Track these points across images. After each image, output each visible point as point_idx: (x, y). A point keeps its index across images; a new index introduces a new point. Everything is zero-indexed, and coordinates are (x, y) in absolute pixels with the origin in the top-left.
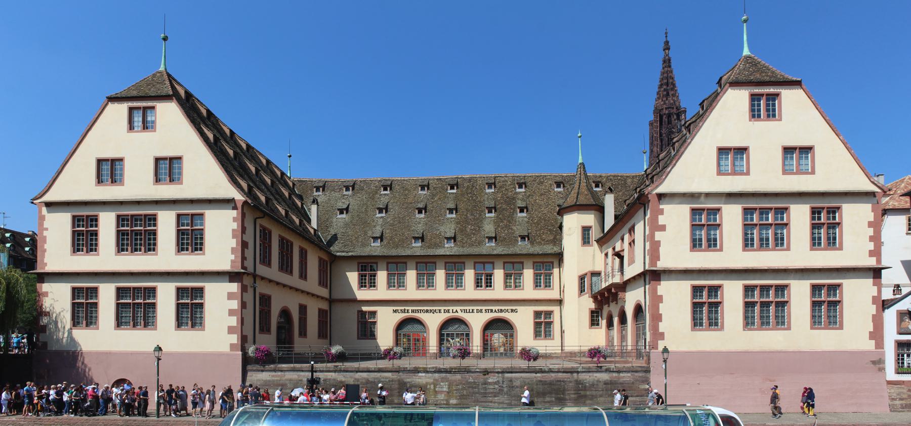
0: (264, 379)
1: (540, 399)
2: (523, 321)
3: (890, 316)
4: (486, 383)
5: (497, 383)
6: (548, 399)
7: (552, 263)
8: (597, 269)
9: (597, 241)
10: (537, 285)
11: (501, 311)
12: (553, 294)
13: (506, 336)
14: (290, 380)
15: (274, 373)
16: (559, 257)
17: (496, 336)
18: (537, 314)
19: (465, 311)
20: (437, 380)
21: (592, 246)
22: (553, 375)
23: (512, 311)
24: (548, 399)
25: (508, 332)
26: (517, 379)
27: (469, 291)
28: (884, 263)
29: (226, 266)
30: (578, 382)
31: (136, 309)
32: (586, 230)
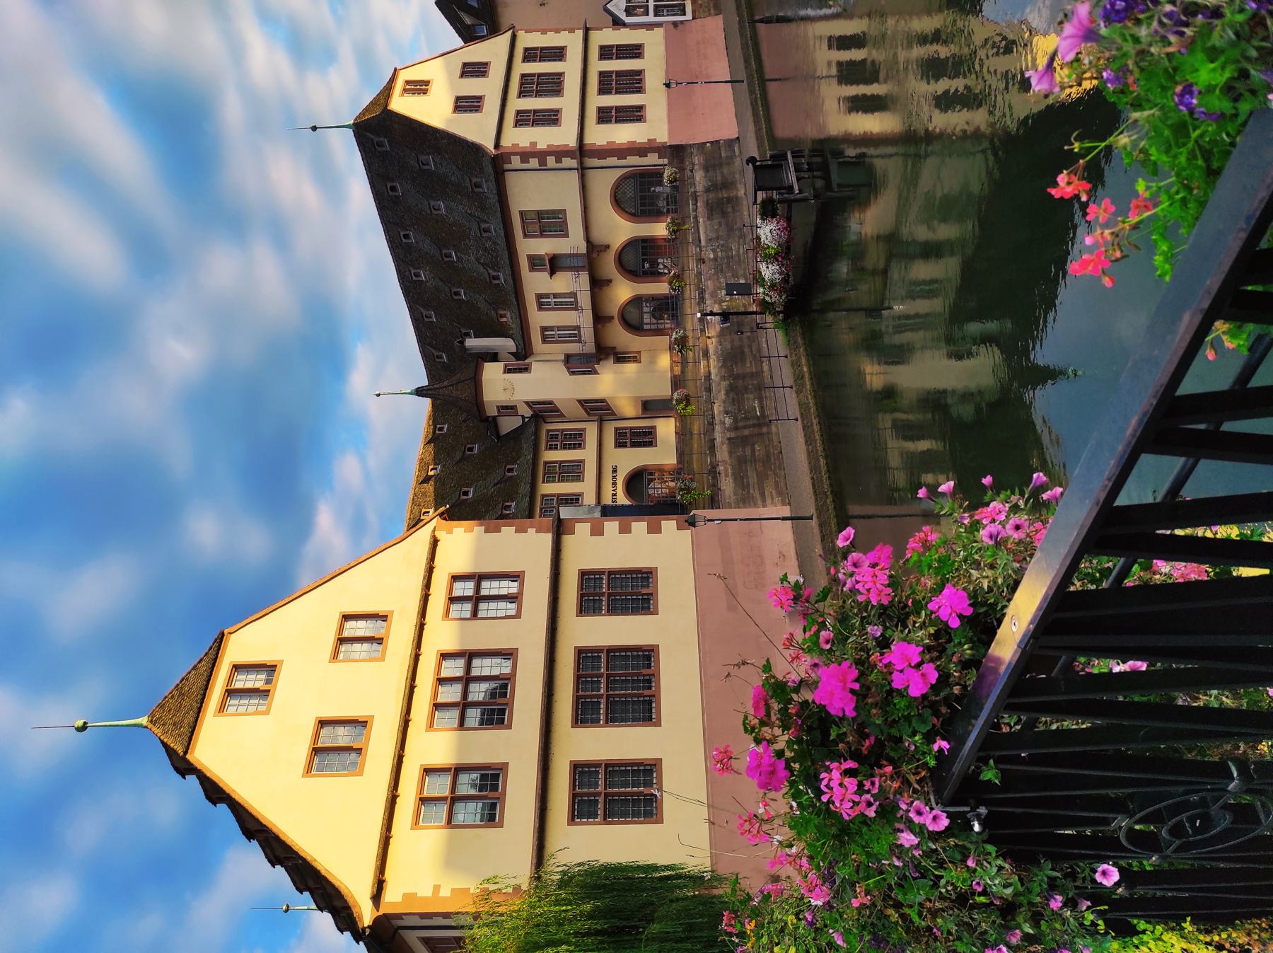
2: (629, 460)
4: (715, 259)
5: (714, 251)
6: (730, 210)
7: (548, 431)
9: (525, 358)
10: (579, 446)
11: (614, 483)
12: (591, 431)
13: (652, 480)
14: (730, 453)
16: (543, 411)
17: (650, 492)
18: (620, 444)
21: (529, 365)
22: (700, 210)
23: (615, 470)
24: (730, 210)
25: (647, 477)
28: (582, 25)
29: (547, 538)
30: (707, 190)
32: (508, 370)
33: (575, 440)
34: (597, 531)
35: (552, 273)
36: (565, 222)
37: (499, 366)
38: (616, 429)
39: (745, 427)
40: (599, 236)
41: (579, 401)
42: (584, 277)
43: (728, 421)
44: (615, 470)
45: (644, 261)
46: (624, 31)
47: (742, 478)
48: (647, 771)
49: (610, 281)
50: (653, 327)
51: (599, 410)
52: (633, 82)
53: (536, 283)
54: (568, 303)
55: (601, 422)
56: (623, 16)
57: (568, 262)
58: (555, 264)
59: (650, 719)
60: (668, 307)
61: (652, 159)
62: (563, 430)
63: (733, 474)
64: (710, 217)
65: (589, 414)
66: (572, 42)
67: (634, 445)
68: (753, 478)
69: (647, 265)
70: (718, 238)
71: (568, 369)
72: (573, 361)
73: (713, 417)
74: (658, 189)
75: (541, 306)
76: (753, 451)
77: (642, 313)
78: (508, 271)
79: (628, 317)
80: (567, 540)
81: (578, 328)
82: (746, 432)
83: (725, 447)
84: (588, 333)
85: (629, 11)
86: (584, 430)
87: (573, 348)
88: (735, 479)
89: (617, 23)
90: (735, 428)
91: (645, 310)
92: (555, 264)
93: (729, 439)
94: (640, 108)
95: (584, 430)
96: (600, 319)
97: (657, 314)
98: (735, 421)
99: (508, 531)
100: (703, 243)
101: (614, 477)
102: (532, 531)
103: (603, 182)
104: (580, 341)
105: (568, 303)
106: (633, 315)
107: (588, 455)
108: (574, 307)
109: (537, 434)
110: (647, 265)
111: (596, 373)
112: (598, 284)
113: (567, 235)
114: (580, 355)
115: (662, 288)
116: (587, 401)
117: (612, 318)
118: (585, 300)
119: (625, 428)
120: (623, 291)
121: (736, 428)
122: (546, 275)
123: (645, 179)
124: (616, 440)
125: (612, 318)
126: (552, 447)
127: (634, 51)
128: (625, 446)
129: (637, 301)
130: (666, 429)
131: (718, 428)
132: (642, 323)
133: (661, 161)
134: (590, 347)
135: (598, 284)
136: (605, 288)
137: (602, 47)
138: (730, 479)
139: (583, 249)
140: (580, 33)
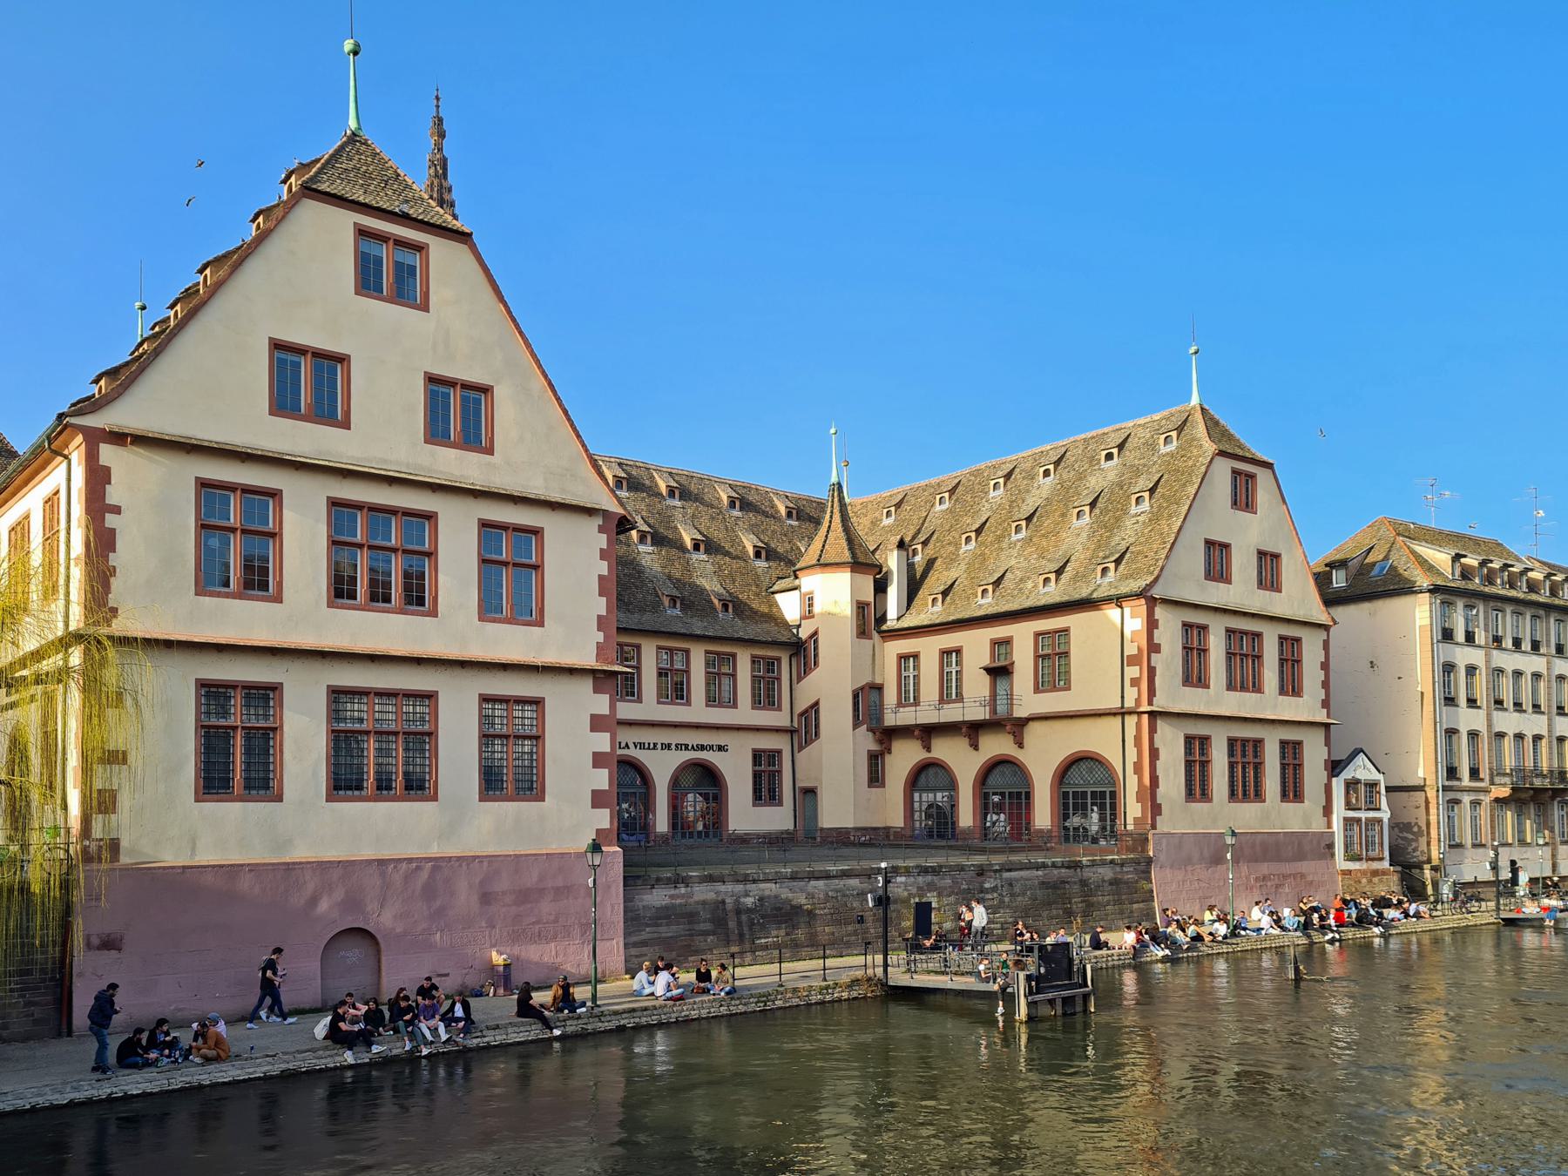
0: (658, 904)
1: (1045, 914)
3: (1338, 786)
5: (994, 889)
7: (779, 660)
8: (878, 681)
9: (880, 632)
11: (702, 748)
12: (780, 718)
13: (706, 797)
14: (704, 903)
15: (673, 892)
17: (690, 797)
18: (757, 756)
19: (642, 746)
20: (920, 888)
22: (1056, 872)
23: (721, 748)
25: (711, 791)
26: (1017, 880)
27: (649, 707)
30: (1084, 883)
31: (379, 753)
33: (765, 696)
34: (597, 723)
35: (989, 670)
36: (1054, 689)
37: (868, 595)
38: (779, 752)
39: (740, 923)
40: (1033, 732)
41: (817, 703)
42: (980, 714)
43: (749, 901)
44: (721, 748)
45: (1003, 794)
46: (1323, 775)
47: (668, 917)
48: (262, 782)
49: (976, 748)
50: (916, 805)
51: (806, 727)
52: (1246, 788)
53: (976, 646)
54: (950, 691)
55: (791, 732)
56: (1348, 774)
57: (1001, 690)
58: (999, 672)
59: (337, 788)
60: (941, 825)
61: (1133, 810)
62: (779, 679)
63: (674, 906)
64: (1044, 884)
65: (801, 715)
66: (1306, 707)
67: (757, 776)
68: (666, 931)
69: (996, 799)
70: (1012, 895)
71: (862, 688)
72: (874, 695)
73: (754, 881)
74: (1095, 816)
75: (946, 653)
76: (706, 933)
77: (934, 790)
78: (991, 611)
79: (931, 771)
80: (587, 684)
81: (917, 703)
82: (732, 924)
83: (711, 896)
84: (906, 717)
85: (1351, 785)
86: (779, 709)
87: (890, 696)
88: (666, 908)
89: (1335, 767)
90: (738, 912)
91: (939, 795)
92: (999, 672)
93: (723, 902)
94: (1205, 796)
95: (779, 709)
96: (928, 733)
97: (934, 811)
98: (749, 910)
99: (601, 606)
100: (1006, 875)
101: (711, 747)
102: (600, 637)
103: (1103, 740)
104: (900, 704)
105: (950, 691)
106: (930, 777)
107: (744, 713)
108: (944, 699)
109: (775, 644)
110: (996, 799)
111: (856, 725)
112: (973, 731)
113: (1037, 690)
114: (882, 704)
115: (966, 817)
116: (817, 712)
117: (929, 750)
118: (952, 714)
119: (780, 764)
120: (964, 761)
121: (738, 912)
122: (986, 661)
123: (1108, 801)
124: (764, 751)
125: (929, 750)
126: (755, 660)
127: (1292, 790)
128: (755, 764)
129: (952, 785)
130: (778, 819)
131: (740, 888)
132: (922, 790)
133: (1130, 821)
134: (890, 720)
135: (973, 731)
136: (966, 740)
137: (1299, 744)
138: (667, 901)
139: (1020, 712)
140: (1321, 716)
